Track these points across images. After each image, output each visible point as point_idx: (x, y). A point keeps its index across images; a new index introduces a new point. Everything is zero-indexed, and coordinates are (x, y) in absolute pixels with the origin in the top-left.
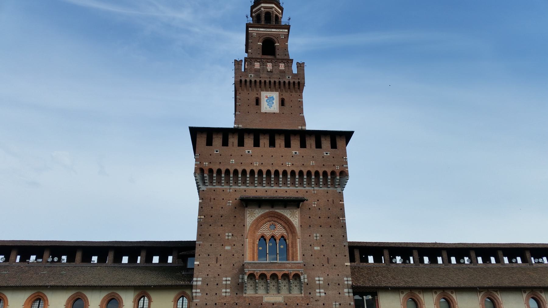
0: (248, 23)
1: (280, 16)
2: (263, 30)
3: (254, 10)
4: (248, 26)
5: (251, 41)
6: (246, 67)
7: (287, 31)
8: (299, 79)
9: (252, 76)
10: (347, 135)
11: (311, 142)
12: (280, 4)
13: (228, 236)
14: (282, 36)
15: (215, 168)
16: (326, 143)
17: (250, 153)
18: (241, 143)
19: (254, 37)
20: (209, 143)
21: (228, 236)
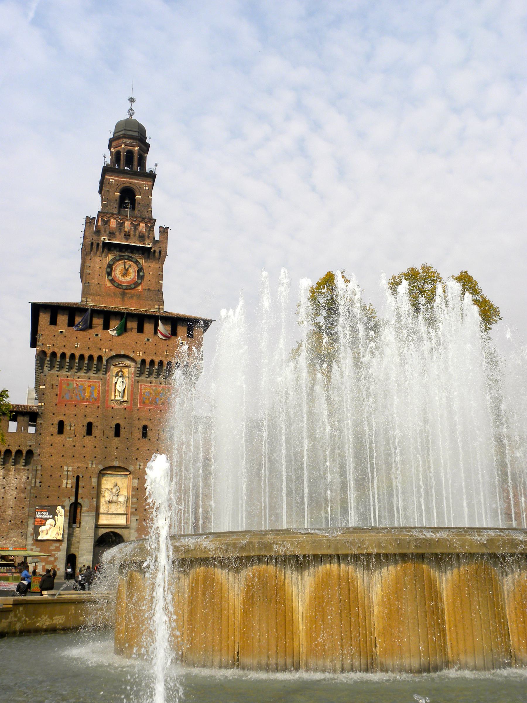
5: (108, 189)
6: (100, 224)
9: (105, 239)
12: (146, 138)
14: (146, 187)
17: (99, 336)
20: (53, 322)
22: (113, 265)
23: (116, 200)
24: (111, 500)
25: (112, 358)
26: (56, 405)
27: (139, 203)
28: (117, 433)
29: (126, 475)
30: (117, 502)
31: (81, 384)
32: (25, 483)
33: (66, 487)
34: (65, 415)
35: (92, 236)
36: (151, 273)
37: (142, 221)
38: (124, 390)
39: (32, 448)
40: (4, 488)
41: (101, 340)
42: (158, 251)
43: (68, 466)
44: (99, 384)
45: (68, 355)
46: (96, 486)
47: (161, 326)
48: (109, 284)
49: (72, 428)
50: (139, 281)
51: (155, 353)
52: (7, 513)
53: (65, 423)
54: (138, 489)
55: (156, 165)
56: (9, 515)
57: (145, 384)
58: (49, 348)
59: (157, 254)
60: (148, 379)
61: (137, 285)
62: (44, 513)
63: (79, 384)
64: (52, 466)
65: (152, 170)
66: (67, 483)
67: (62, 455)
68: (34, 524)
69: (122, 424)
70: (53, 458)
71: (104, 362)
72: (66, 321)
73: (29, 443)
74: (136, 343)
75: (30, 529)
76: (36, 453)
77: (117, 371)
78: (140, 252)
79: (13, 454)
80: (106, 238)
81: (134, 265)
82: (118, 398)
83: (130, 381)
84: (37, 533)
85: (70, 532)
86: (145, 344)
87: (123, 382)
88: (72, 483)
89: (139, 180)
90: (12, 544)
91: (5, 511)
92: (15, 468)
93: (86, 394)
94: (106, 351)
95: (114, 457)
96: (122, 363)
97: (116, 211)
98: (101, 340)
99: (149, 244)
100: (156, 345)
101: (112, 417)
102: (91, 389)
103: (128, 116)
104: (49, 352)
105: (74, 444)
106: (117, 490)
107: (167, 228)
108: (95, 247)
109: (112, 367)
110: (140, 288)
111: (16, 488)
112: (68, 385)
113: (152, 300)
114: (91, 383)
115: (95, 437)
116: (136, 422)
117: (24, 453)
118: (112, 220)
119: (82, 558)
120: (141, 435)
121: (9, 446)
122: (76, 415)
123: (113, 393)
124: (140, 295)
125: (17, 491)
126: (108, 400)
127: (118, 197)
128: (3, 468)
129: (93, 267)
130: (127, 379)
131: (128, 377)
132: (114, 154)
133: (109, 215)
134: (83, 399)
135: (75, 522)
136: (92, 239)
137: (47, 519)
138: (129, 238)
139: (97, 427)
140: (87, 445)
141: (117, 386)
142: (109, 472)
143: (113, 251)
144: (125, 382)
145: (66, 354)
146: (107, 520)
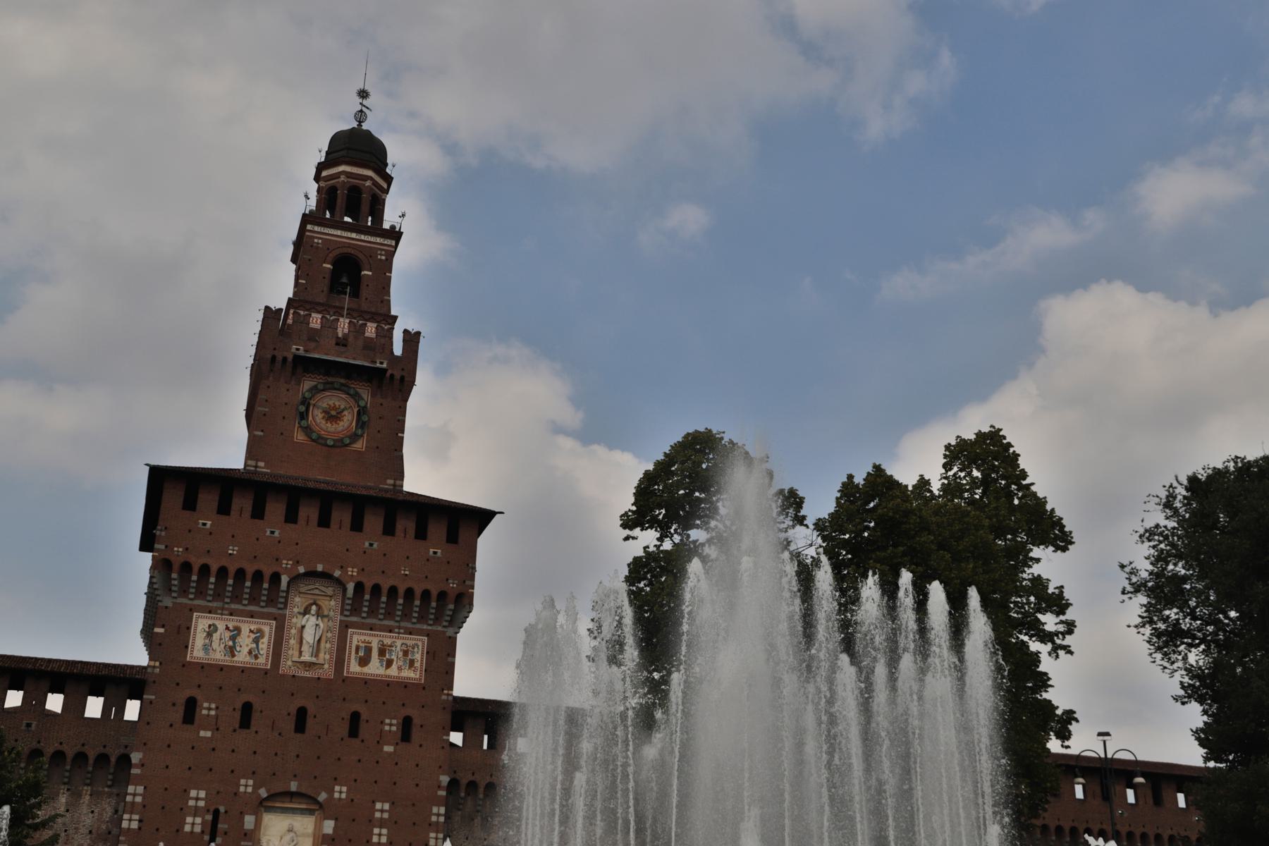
0: (307, 212)
2: (339, 233)
3: (324, 174)
4: (306, 219)
5: (310, 257)
6: (290, 321)
7: (393, 243)
9: (297, 349)
10: (482, 518)
11: (406, 525)
13: (209, 709)
14: (381, 255)
15: (196, 563)
16: (437, 530)
17: (277, 534)
18: (258, 513)
19: (317, 248)
21: (209, 709)
22: (311, 399)
26: (184, 666)
28: (300, 726)
29: (310, 812)
34: (199, 686)
37: (370, 319)
38: (319, 641)
41: (279, 542)
42: (399, 377)
45: (214, 568)
48: (300, 437)
49: (213, 713)
50: (360, 432)
51: (383, 572)
54: (333, 840)
55: (403, 215)
60: (369, 621)
61: (355, 437)
65: (395, 224)
67: (188, 766)
72: (215, 505)
74: (347, 550)
77: (307, 603)
79: (91, 761)
80: (301, 348)
81: (352, 403)
82: (307, 657)
86: (365, 552)
87: (317, 625)
88: (203, 823)
92: (92, 790)
96: (317, 588)
98: (279, 542)
99: (382, 363)
100: (385, 555)
103: (355, 124)
107: (418, 333)
108: (278, 364)
110: (359, 445)
111: (90, 832)
117: (113, 760)
118: (313, 315)
121: (83, 745)
122: (221, 688)
125: (91, 839)
128: (68, 790)
130: (326, 620)
132: (324, 192)
133: (308, 307)
136: (275, 349)
144: (322, 625)
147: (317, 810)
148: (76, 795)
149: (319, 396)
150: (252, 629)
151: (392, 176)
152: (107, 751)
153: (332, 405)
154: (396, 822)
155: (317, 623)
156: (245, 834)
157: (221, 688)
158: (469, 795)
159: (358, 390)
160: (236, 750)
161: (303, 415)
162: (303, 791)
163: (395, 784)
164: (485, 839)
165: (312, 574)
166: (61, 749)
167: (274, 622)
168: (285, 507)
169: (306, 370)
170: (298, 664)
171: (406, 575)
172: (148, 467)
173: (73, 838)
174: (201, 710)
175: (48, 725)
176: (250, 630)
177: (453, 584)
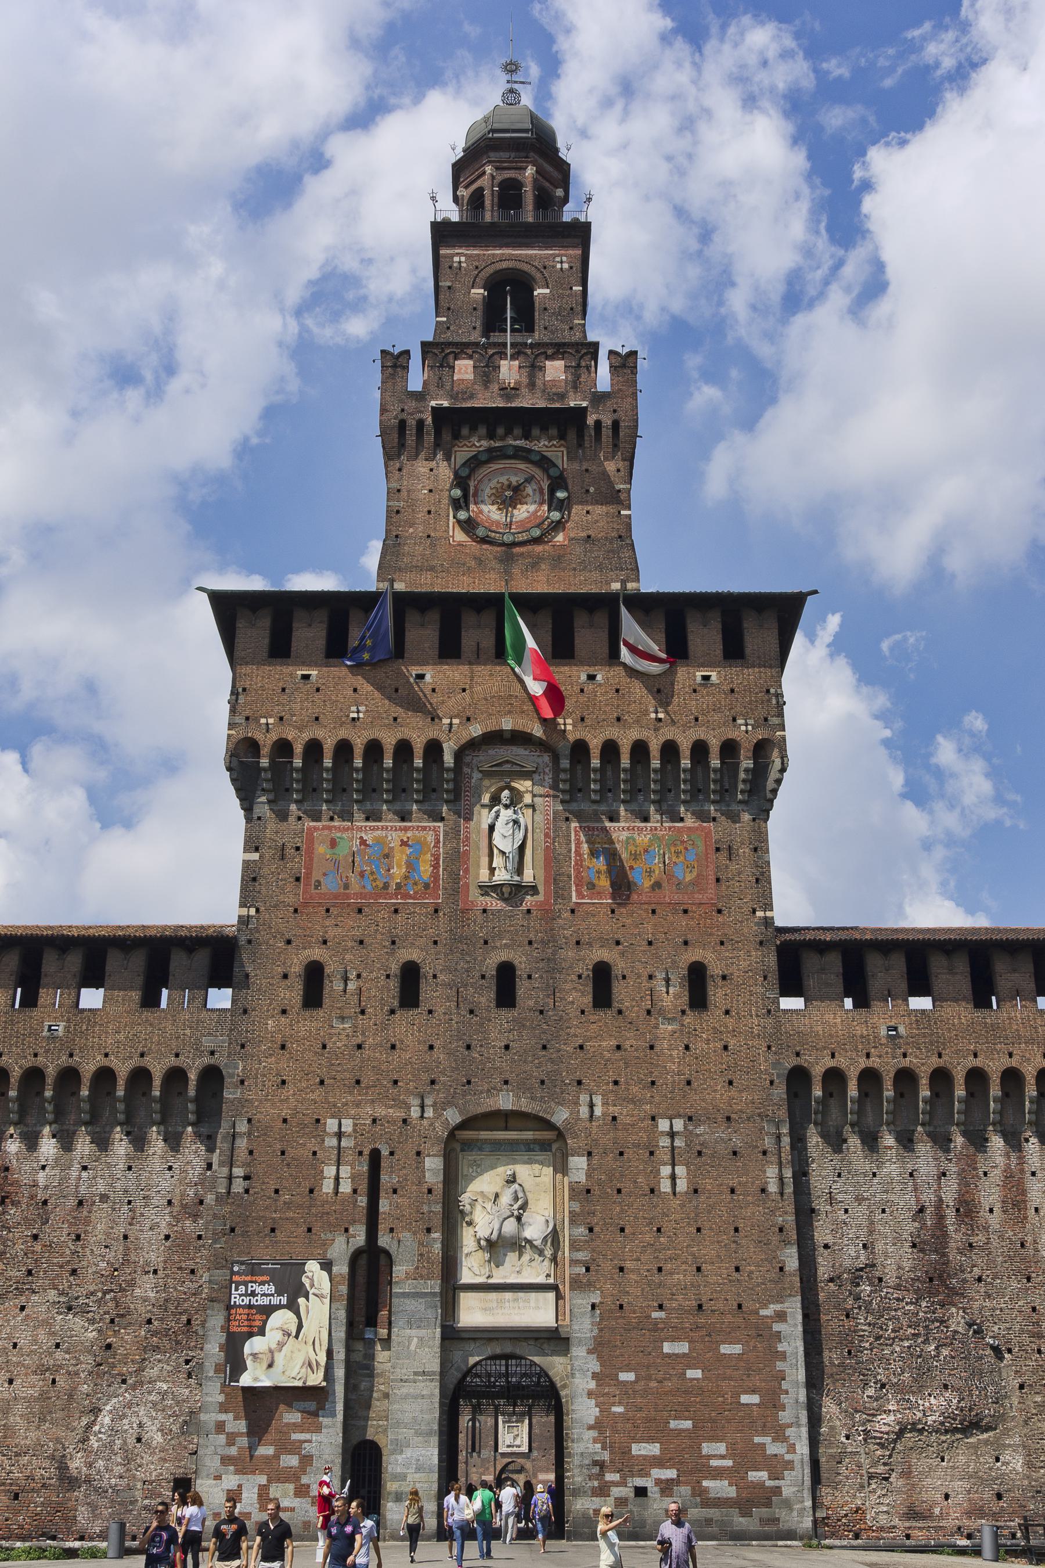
0: (439, 220)
1: (560, 192)
5: (449, 284)
7: (579, 241)
8: (615, 411)
12: (557, 150)
14: (562, 262)
22: (469, 477)
23: (475, 309)
24: (494, 1237)
25: (473, 745)
26: (296, 911)
27: (545, 309)
29: (544, 1146)
30: (517, 1244)
31: (375, 838)
32: (201, 1182)
33: (336, 1192)
34: (325, 942)
35: (401, 401)
36: (592, 489)
38: (522, 848)
39: (220, 1060)
40: (129, 1202)
42: (609, 422)
43: (338, 1116)
44: (437, 836)
46: (441, 1186)
47: (630, 627)
48: (460, 536)
49: (351, 986)
50: (556, 515)
52: (137, 1291)
53: (327, 971)
54: (588, 1191)
56: (145, 1300)
57: (592, 825)
58: (268, 731)
59: (606, 433)
60: (603, 808)
62: (258, 1289)
63: (369, 837)
64: (285, 1121)
66: (337, 1179)
68: (226, 1328)
69: (521, 961)
70: (290, 1090)
71: (448, 759)
72: (321, 642)
73: (208, 1043)
75: (213, 1349)
76: (232, 1076)
78: (553, 432)
79: (157, 1082)
81: (538, 473)
82: (502, 876)
83: (539, 817)
84: (235, 1363)
85: (357, 1357)
86: (582, 691)
88: (353, 1178)
89: (540, 248)
90: (155, 1404)
91: (132, 1284)
93: (394, 871)
94: (451, 724)
95: (497, 1080)
97: (476, 336)
100: (617, 691)
101: (486, 942)
102: (408, 851)
104: (266, 742)
105: (359, 1040)
106: (516, 1199)
107: (633, 354)
109: (476, 775)
111: (170, 1202)
112: (333, 844)
113: (600, 568)
114: (409, 834)
115: (430, 1012)
116: (569, 954)
117: (193, 1076)
119: (400, 1458)
120: (588, 999)
121: (142, 1055)
122: (361, 942)
123: (484, 860)
124: (560, 557)
126: (467, 885)
127: (481, 297)
129: (408, 491)
131: (532, 806)
132: (465, 201)
134: (386, 886)
135: (372, 1321)
136: (403, 410)
137: (268, 1311)
138: (518, 395)
139: (435, 976)
140: (402, 1042)
141: (496, 835)
142: (485, 1135)
143: (467, 438)
144: (522, 821)
145: (323, 741)
146: (485, 1309)
147: (555, 1141)
148: (139, 1142)
149: (483, 471)
150: (405, 839)
151: (568, 161)
152: (182, 1062)
153: (506, 483)
154: (700, 1153)
155: (514, 817)
156: (430, 1191)
157: (361, 942)
158: (831, 1095)
159: (544, 453)
160: (398, 1046)
161: (459, 503)
162: (525, 1105)
163: (689, 1083)
164: (874, 1175)
165: (494, 738)
166: (107, 1064)
167: (440, 824)
168: (437, 633)
169: (457, 436)
170: (489, 890)
171: (660, 720)
172: (205, 596)
173: (142, 1215)
174: (331, 982)
175: (84, 1027)
176: (402, 840)
177: (746, 725)
